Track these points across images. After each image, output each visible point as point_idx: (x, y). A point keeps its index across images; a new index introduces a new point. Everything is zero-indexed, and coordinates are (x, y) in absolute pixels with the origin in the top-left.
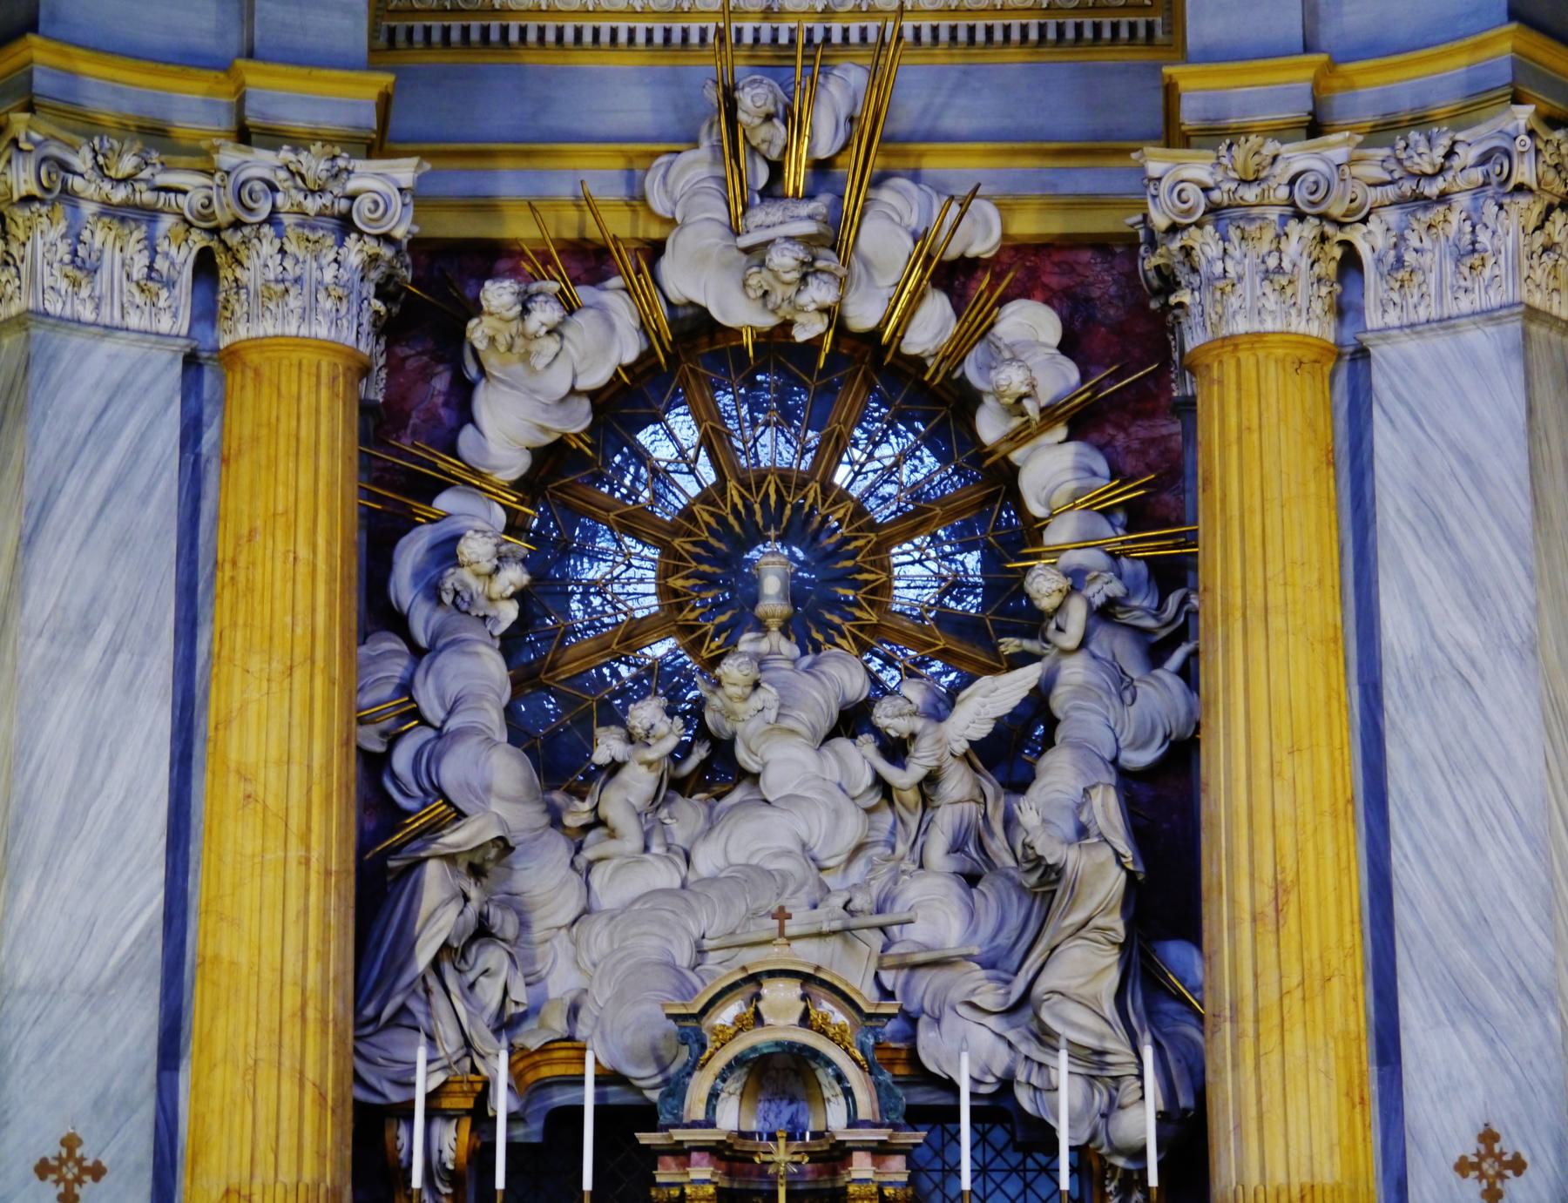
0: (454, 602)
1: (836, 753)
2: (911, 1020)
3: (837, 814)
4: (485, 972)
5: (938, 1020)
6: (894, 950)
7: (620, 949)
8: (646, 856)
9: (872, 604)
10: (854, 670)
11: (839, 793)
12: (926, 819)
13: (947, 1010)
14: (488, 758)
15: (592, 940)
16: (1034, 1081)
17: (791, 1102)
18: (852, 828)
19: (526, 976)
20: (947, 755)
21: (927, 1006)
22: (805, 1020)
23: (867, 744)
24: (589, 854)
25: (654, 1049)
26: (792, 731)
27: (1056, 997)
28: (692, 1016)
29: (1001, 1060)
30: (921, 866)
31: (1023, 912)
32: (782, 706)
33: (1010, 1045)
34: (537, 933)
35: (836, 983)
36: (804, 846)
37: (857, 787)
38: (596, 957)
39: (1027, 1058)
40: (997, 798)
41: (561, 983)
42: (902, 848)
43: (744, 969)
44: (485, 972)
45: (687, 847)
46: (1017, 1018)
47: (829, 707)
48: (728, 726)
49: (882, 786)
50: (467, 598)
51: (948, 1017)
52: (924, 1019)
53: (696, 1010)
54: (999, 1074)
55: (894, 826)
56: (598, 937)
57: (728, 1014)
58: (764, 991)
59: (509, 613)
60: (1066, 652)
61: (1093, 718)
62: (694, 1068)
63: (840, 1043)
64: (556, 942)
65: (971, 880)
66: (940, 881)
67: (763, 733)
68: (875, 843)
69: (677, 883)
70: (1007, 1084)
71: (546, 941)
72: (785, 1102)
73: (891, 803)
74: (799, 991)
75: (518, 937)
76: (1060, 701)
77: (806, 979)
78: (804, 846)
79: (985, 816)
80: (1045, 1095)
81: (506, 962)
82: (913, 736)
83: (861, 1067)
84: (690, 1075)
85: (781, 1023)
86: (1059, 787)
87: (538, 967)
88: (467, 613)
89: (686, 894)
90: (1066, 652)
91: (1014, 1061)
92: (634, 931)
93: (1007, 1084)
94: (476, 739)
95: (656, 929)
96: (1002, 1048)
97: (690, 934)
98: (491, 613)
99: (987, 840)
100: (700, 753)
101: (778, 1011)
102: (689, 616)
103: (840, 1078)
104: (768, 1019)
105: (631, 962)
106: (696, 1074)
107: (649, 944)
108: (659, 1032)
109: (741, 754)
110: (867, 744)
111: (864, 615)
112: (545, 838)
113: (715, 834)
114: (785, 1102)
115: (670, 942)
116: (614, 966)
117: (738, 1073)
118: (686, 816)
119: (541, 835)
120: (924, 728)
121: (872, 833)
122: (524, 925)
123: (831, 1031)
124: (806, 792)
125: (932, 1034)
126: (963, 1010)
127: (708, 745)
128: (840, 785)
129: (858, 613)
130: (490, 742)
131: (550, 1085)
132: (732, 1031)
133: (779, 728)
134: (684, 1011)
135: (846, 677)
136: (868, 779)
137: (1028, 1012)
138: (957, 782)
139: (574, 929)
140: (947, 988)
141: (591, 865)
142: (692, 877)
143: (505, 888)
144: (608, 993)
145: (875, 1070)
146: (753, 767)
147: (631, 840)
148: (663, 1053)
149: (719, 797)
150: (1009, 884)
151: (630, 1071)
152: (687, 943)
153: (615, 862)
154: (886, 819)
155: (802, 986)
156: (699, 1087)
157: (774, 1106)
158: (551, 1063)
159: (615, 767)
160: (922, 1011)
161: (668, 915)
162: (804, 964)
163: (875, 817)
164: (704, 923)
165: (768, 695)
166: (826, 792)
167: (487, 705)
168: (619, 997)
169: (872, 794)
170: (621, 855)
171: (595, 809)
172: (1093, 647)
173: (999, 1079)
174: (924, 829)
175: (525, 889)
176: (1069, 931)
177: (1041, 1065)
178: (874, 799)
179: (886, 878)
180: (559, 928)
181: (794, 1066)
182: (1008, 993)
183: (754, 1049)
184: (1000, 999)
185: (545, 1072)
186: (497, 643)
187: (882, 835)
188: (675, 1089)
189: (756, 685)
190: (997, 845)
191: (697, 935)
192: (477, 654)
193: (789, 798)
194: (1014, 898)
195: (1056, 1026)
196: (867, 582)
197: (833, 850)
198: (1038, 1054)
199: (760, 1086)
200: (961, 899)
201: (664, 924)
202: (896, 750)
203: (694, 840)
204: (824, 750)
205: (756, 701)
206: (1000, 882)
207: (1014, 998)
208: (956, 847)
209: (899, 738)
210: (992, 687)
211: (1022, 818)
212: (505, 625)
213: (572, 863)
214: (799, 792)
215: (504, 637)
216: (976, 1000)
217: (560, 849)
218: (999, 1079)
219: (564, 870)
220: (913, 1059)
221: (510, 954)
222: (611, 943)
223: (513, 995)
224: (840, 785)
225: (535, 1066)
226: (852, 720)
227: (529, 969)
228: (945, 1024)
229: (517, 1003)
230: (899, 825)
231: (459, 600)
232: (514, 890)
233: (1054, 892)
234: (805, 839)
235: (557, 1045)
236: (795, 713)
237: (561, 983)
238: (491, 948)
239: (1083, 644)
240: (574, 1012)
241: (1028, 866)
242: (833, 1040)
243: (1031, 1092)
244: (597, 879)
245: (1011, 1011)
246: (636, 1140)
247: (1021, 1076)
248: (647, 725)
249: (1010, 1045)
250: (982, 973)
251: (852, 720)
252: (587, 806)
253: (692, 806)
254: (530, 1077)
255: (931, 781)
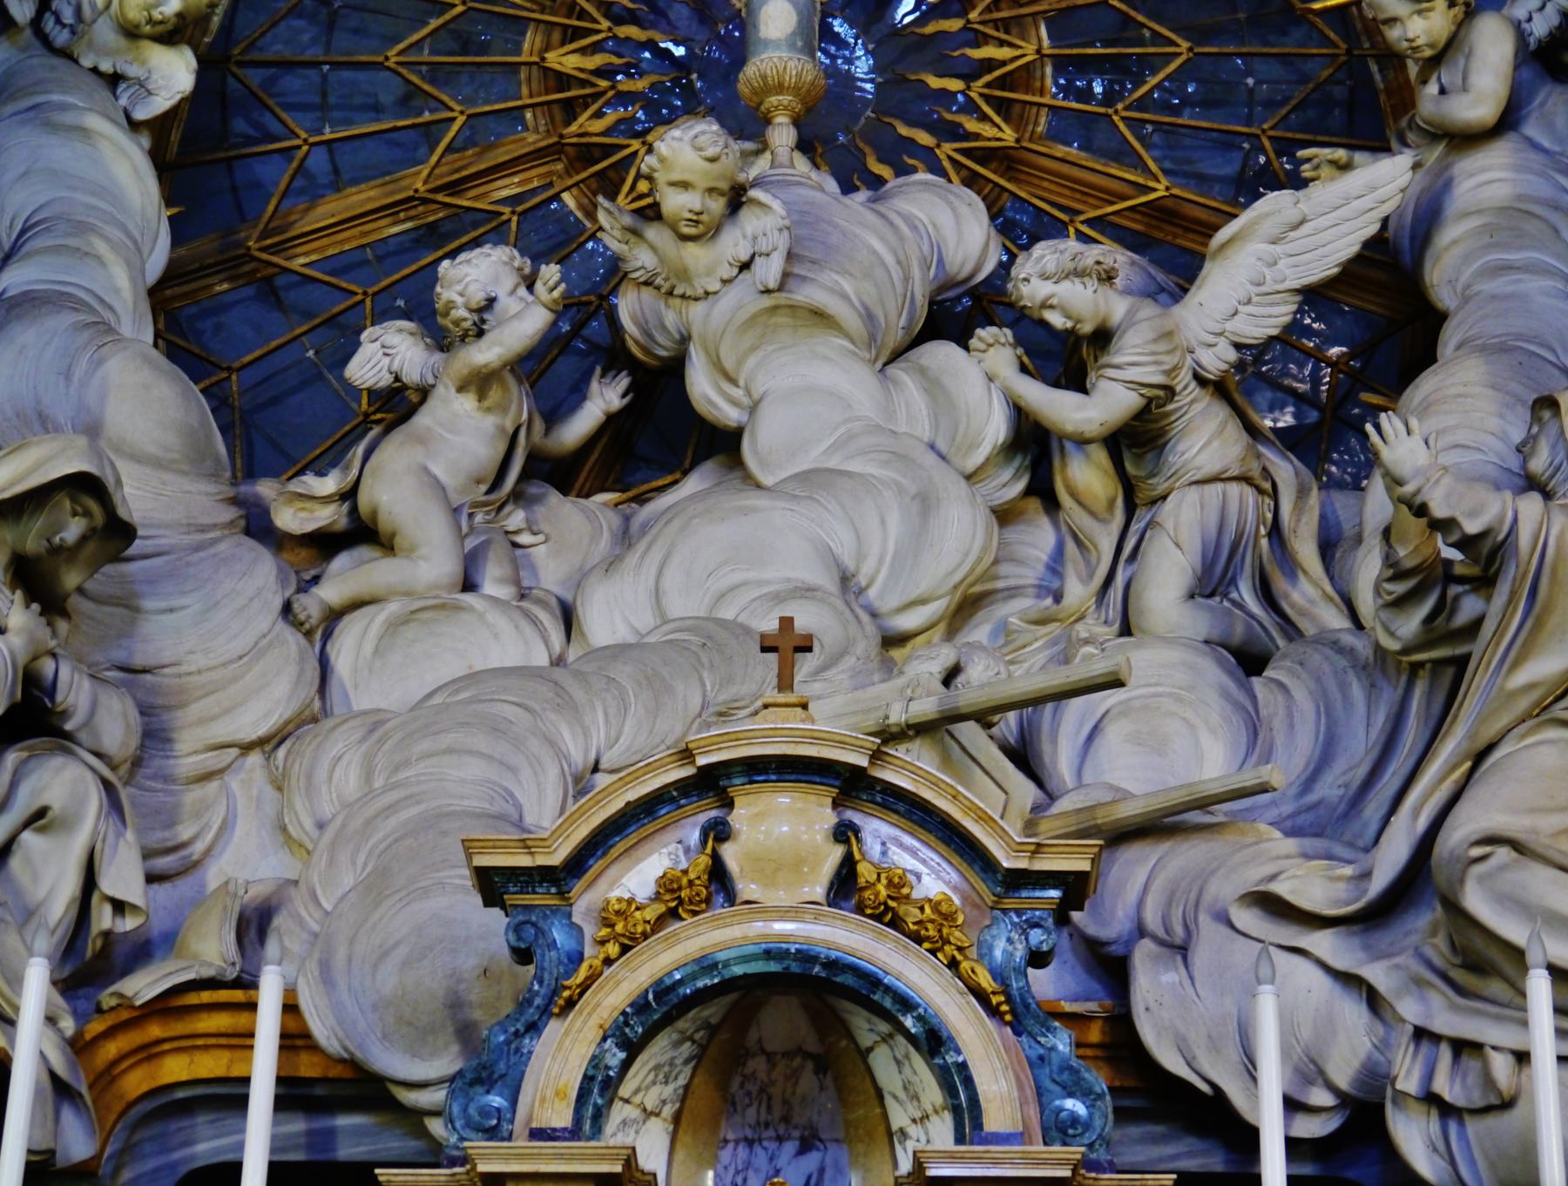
0: (36, 23)
1: (923, 372)
2: (1110, 967)
3: (925, 503)
4: (37, 818)
5: (1182, 950)
6: (1064, 805)
7: (386, 789)
8: (468, 598)
9: (1003, 107)
10: (964, 210)
11: (931, 459)
12: (1136, 527)
13: (1204, 919)
14: (100, 363)
15: (321, 774)
16: (1443, 1086)
17: (805, 1147)
18: (960, 536)
19: (147, 854)
20: (1184, 378)
21: (1152, 920)
22: (845, 886)
23: (996, 350)
24: (331, 592)
25: (455, 1004)
26: (820, 317)
27: (1503, 854)
28: (547, 875)
29: (1350, 1045)
30: (1126, 630)
31: (1381, 718)
32: (790, 256)
33: (1374, 1000)
34: (188, 753)
35: (927, 794)
36: (845, 579)
37: (974, 446)
38: (327, 809)
39: (1420, 1034)
40: (1302, 493)
41: (244, 862)
42: (1078, 591)
43: (686, 755)
44: (37, 818)
45: (568, 597)
46: (1384, 938)
47: (907, 279)
48: (670, 319)
49: (1033, 443)
50: (68, 16)
51: (1210, 941)
52: (1143, 958)
53: (556, 859)
54: (1343, 1082)
55: (1059, 553)
56: (337, 769)
57: (638, 876)
58: (739, 817)
59: (173, 74)
60: (1465, 139)
61: (1534, 285)
62: (546, 1012)
63: (929, 934)
64: (234, 782)
65: (1250, 660)
66: (1173, 655)
67: (753, 320)
68: (1013, 592)
69: (541, 659)
70: (1364, 1113)
71: (207, 777)
72: (790, 1147)
73: (1052, 504)
74: (829, 818)
75: (137, 763)
76: (1448, 270)
77: (852, 786)
78: (845, 579)
79: (1276, 531)
80: (1473, 1126)
81: (94, 799)
82: (1103, 337)
83: (993, 1011)
84: (534, 1028)
85: (780, 897)
86: (1461, 437)
87: (185, 833)
88: (67, 55)
89: (558, 673)
90: (1465, 139)
91: (1383, 1046)
92: (425, 745)
93: (1364, 1113)
94: (68, 319)
95: (481, 742)
96: (1353, 1012)
97: (561, 755)
98: (132, 71)
99: (1280, 583)
100: (605, 398)
101: (774, 867)
102: (589, 125)
103: (934, 1042)
104: (747, 888)
105: (414, 811)
106: (553, 1028)
107: (461, 779)
108: (469, 964)
109: (704, 389)
110: (996, 350)
111: (987, 130)
112: (222, 547)
113: (632, 559)
114: (790, 1147)
115: (512, 769)
116: (369, 823)
117: (659, 1050)
118: (570, 527)
119: (214, 542)
120: (1131, 313)
121: (1004, 569)
122: (154, 735)
123: (911, 915)
124: (852, 471)
125: (1172, 977)
126: (1247, 918)
127: (624, 382)
128: (932, 447)
129: (971, 125)
130: (104, 329)
131: (187, 1108)
132: (651, 914)
133: (788, 310)
134: (524, 861)
135: (945, 218)
136: (997, 428)
137: (1423, 921)
138: (1205, 439)
139: (281, 753)
140: (1203, 877)
141: (334, 616)
142: (572, 655)
143: (119, 655)
144: (348, 880)
145: (1029, 1023)
146: (730, 415)
147: (431, 558)
148: (477, 1015)
149: (641, 500)
150: (1342, 662)
151: (392, 1062)
152: (552, 773)
153: (393, 608)
154: (1038, 537)
155: (836, 804)
156: (559, 1059)
157: (761, 1157)
158: (190, 1044)
159: (398, 404)
160: (1141, 931)
161: (510, 712)
162: (842, 744)
163: (1015, 534)
164: (599, 737)
165: (763, 225)
166: (900, 458)
167: (101, 247)
168: (376, 887)
169: (1007, 474)
170: (408, 594)
171: (349, 495)
172: (1531, 129)
173: (1344, 1099)
174: (1128, 552)
175: (166, 657)
176: (1523, 704)
177: (1462, 1047)
178: (1010, 485)
179: (1041, 658)
180: (247, 748)
181: (812, 1045)
182: (1366, 875)
183: (706, 965)
184: (1341, 890)
185: (175, 1069)
186: (146, 142)
187: (1030, 575)
188: (491, 1068)
189: (737, 199)
190: (1308, 596)
191: (579, 757)
192: (84, 133)
193: (813, 481)
194: (1357, 691)
195: (1513, 930)
196: (989, 65)
197: (917, 582)
198: (1449, 1020)
199: (730, 1105)
200: (1225, 695)
201: (497, 728)
202: (1067, 357)
203: (580, 580)
204: (893, 370)
205: (733, 244)
206: (1316, 658)
207: (1380, 882)
208: (1210, 583)
209: (1071, 332)
210: (1293, 215)
211: (1386, 453)
212: (160, 104)
213: (287, 609)
214: (833, 463)
215: (158, 128)
216: (1281, 888)
217: (258, 577)
218: (1344, 1099)
219: (266, 617)
220: (1121, 1045)
221: (107, 785)
222: (368, 776)
223: (109, 884)
224: (932, 447)
225: (149, 1053)
226: (959, 311)
227: (158, 838)
228: (1201, 955)
229: (119, 907)
230: (1070, 546)
231: (49, 24)
232: (139, 661)
233: (1461, 663)
234: (849, 563)
235: (206, 996)
236: (828, 277)
237: (244, 862)
238: (58, 761)
239: (1508, 121)
240: (254, 926)
241: (1400, 588)
242: (918, 940)
243: (1434, 1126)
244: (347, 648)
245: (1372, 919)
246: (376, 1176)
247: (1409, 1083)
248: (478, 298)
249: (1374, 1000)
250: (1291, 845)
251: (959, 311)
252: (329, 484)
253: (590, 516)
254: (136, 1082)
255: (1138, 441)
